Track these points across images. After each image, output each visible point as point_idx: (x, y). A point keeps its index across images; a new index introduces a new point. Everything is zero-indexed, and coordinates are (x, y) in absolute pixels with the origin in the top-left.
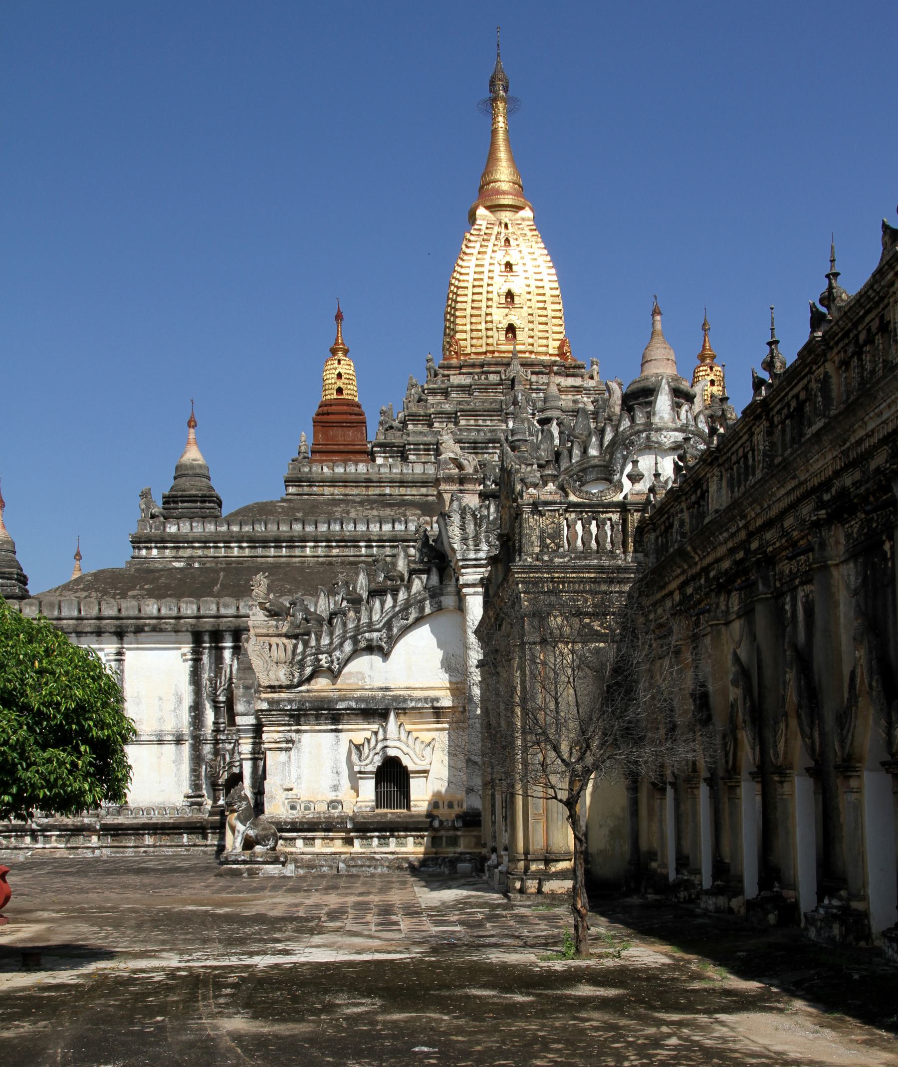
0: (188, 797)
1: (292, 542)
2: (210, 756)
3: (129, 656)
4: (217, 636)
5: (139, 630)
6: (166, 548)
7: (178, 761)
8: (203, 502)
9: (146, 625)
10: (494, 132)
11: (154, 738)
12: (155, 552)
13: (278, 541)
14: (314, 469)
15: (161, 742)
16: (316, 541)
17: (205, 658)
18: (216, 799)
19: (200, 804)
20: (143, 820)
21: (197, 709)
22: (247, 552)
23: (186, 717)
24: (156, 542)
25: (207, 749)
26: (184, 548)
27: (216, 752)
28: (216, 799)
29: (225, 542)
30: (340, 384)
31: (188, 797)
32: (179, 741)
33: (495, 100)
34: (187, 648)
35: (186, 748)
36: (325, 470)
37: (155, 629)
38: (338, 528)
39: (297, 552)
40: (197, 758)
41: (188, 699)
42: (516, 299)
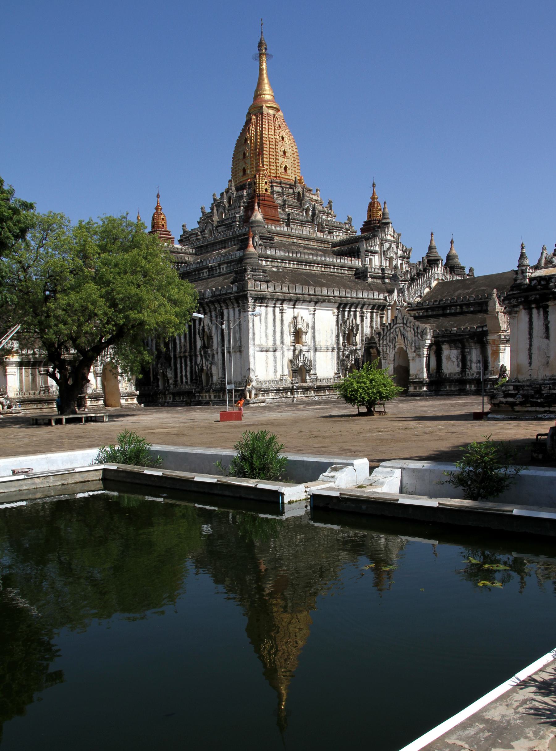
0: (336, 374)
1: (311, 263)
2: (341, 357)
3: (317, 312)
4: (345, 305)
5: (324, 301)
6: (268, 261)
7: (332, 359)
8: (270, 240)
9: (326, 299)
10: (261, 70)
11: (326, 349)
12: (264, 262)
13: (306, 262)
14: (269, 227)
15: (327, 350)
16: (318, 264)
17: (340, 316)
18: (345, 375)
19: (340, 377)
20: (324, 384)
21: (338, 336)
22: (295, 266)
23: (334, 340)
24: (265, 258)
25: (341, 353)
26: (275, 262)
27: (343, 355)
28: (345, 375)
29: (289, 261)
30: (266, 187)
31: (336, 374)
32: (333, 350)
33: (261, 54)
34: (335, 310)
35: (335, 353)
36: (273, 228)
37: (329, 301)
38: (324, 259)
39: (311, 268)
40: (338, 357)
41: (335, 333)
42: (287, 155)
